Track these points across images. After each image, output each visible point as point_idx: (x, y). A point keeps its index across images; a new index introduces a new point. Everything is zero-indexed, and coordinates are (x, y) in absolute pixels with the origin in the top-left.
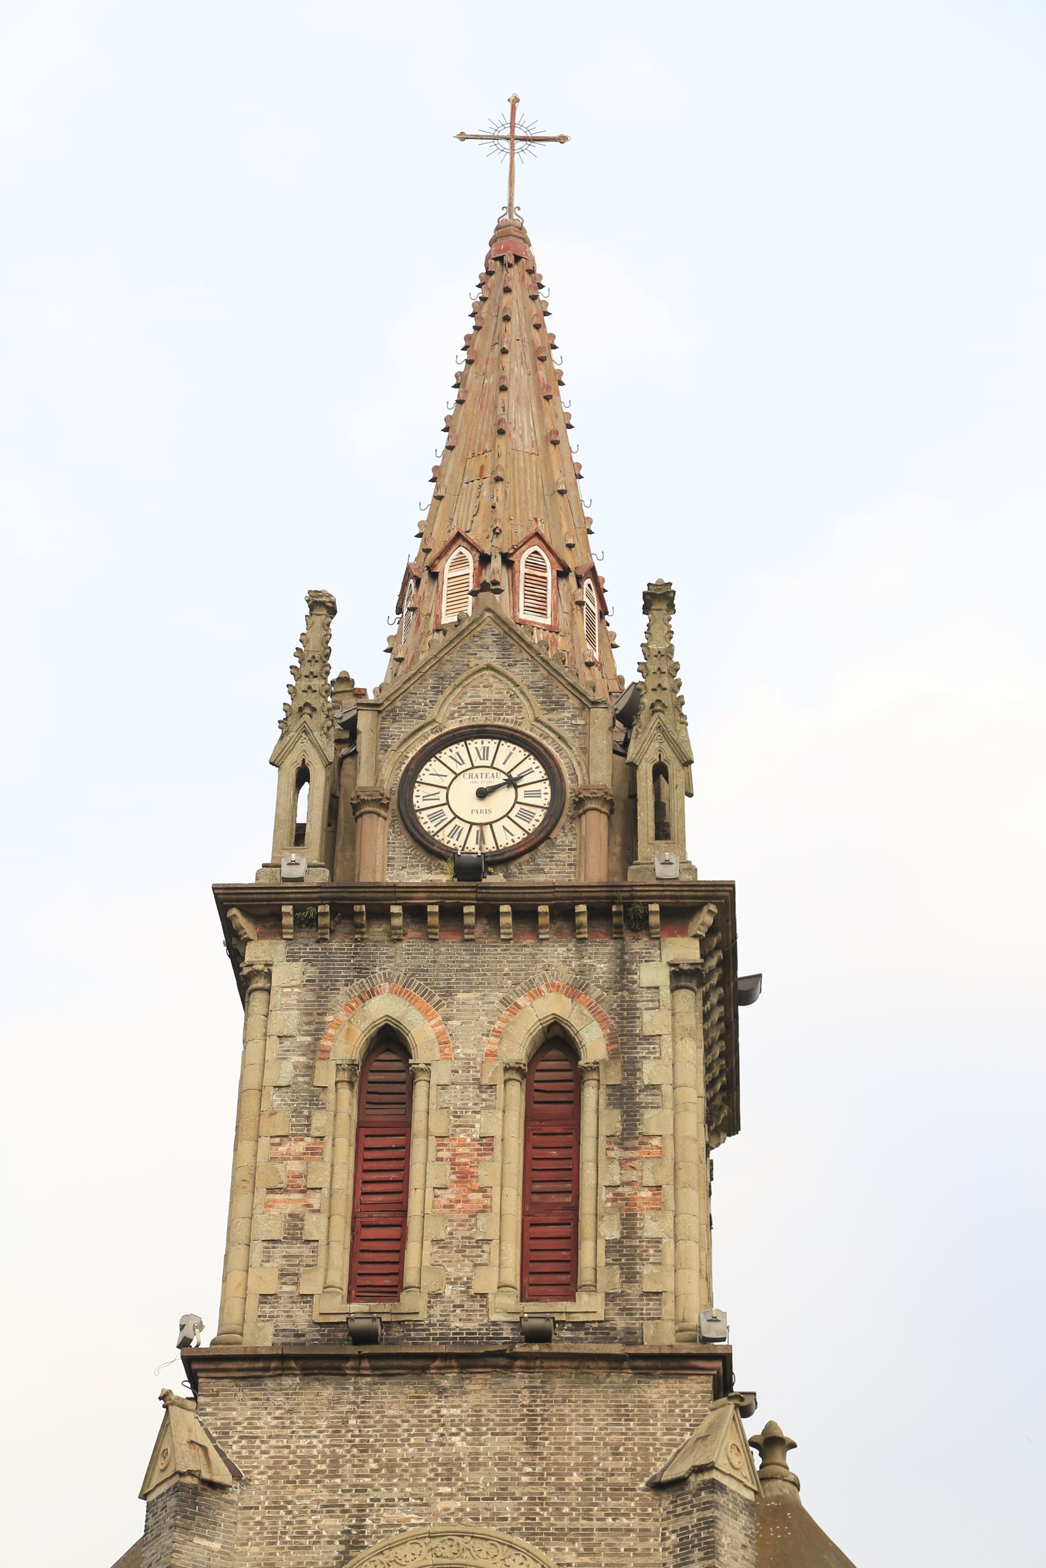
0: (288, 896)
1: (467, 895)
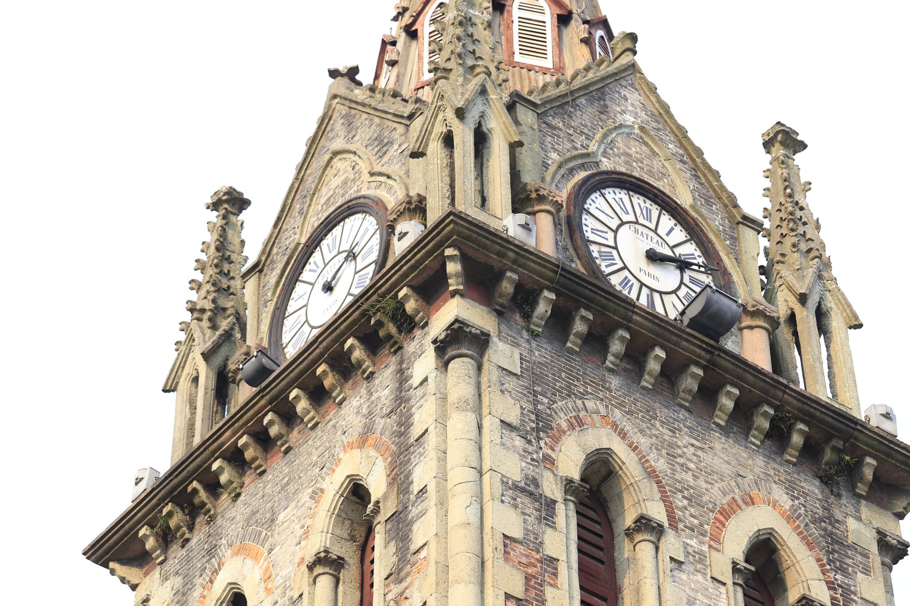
0: (136, 518)
1: (259, 405)
